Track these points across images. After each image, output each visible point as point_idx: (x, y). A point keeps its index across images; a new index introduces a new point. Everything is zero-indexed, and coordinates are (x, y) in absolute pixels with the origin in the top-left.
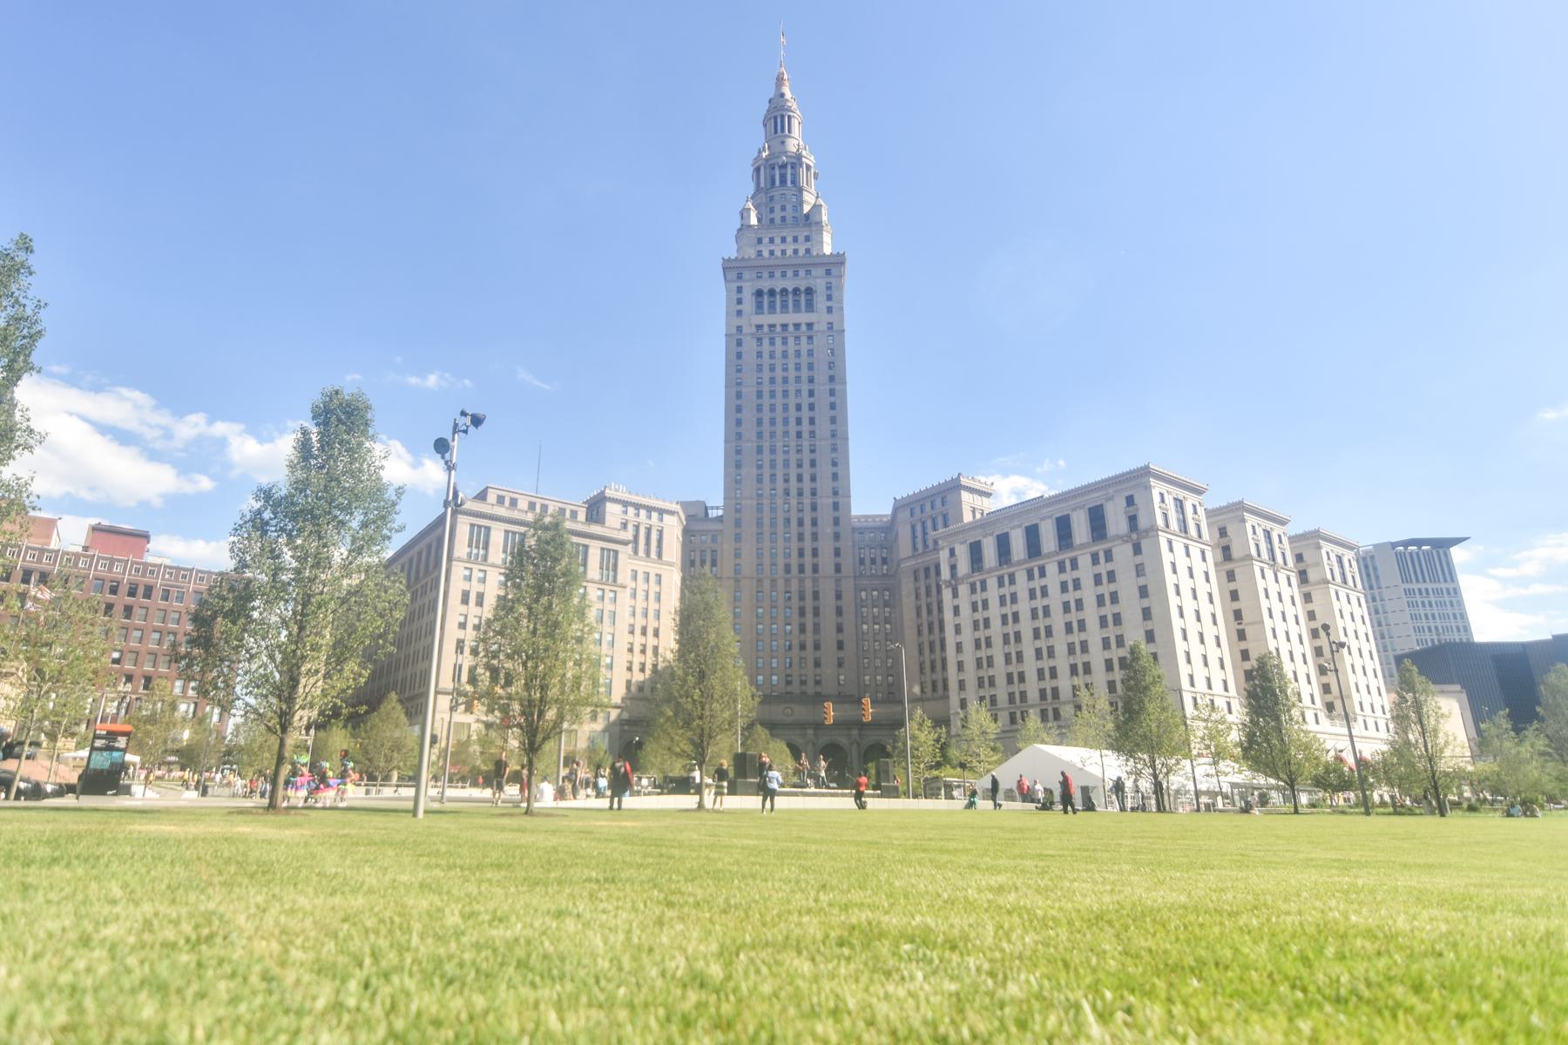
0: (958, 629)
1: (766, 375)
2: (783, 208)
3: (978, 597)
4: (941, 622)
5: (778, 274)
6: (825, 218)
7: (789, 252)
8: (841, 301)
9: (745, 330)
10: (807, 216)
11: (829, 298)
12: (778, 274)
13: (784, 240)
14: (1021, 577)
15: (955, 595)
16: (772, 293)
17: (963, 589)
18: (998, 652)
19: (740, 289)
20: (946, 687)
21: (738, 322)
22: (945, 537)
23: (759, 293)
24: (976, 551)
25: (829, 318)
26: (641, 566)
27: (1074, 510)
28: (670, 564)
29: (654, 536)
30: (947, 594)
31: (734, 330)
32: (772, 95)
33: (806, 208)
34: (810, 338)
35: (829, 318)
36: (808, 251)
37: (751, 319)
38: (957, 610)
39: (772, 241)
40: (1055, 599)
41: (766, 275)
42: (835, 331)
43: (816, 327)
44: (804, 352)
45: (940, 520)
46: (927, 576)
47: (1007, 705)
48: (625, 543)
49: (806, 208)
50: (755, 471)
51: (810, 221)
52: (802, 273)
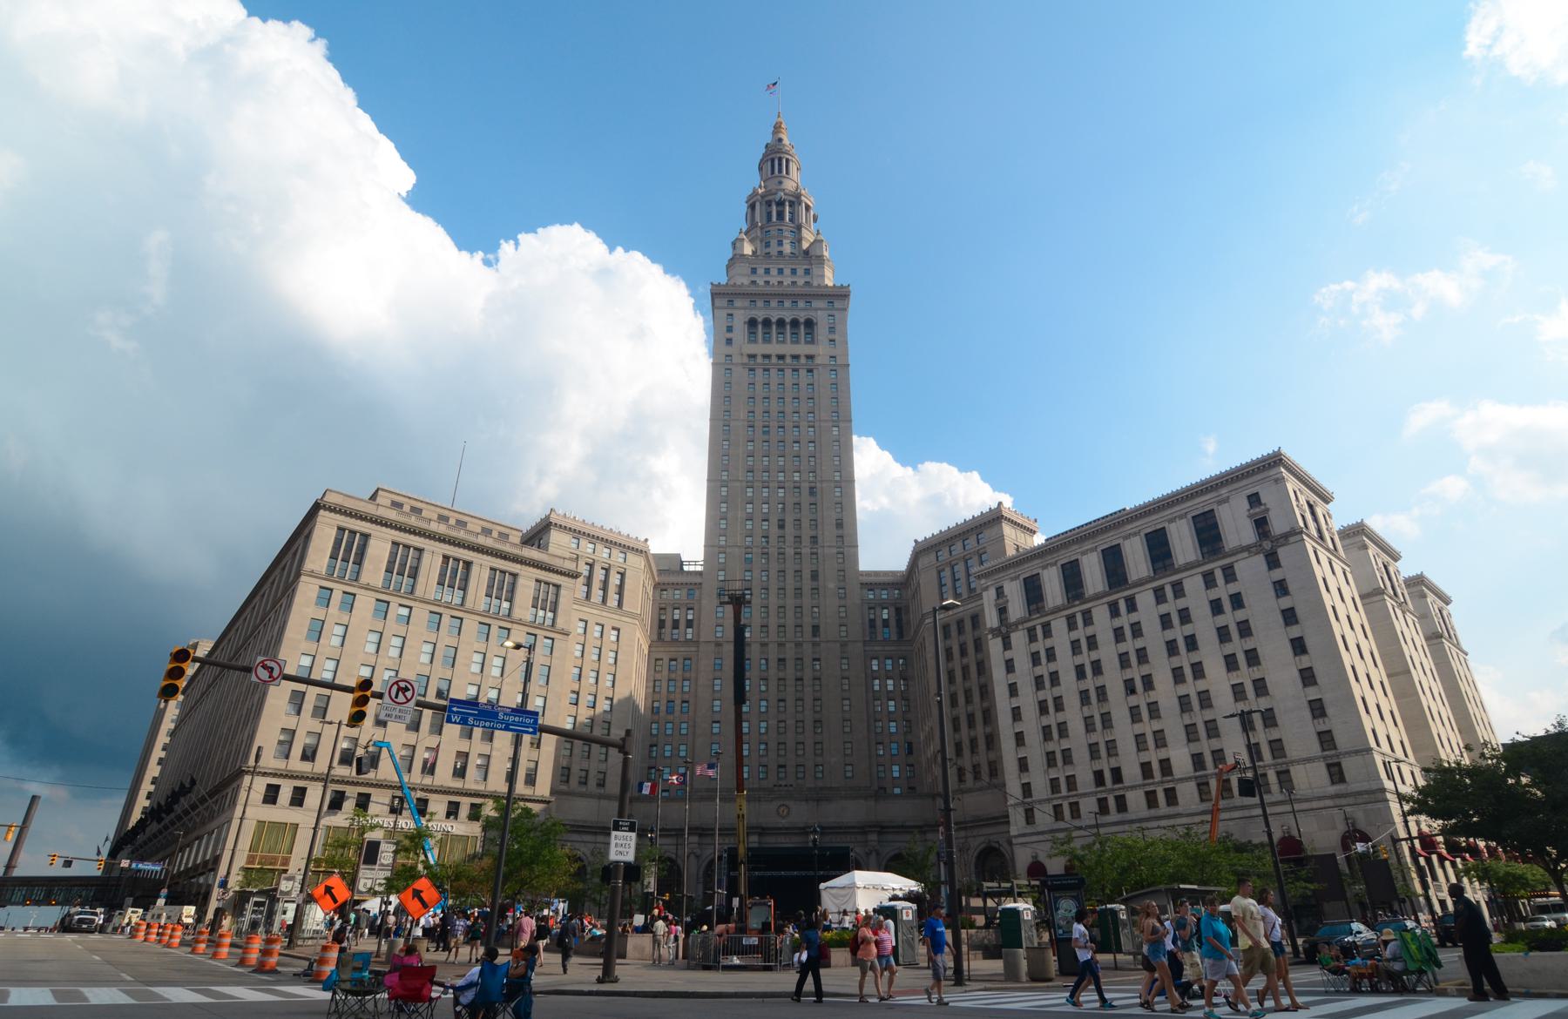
0: (1013, 690)
2: (780, 243)
3: (1040, 646)
5: (774, 303)
6: (826, 254)
9: (736, 359)
10: (806, 252)
11: (832, 330)
12: (774, 303)
14: (1101, 614)
15: (1007, 645)
16: (767, 323)
17: (1019, 638)
18: (1073, 715)
21: (729, 350)
22: (987, 575)
23: (752, 323)
24: (1033, 590)
26: (593, 613)
27: (1171, 521)
28: (632, 615)
29: (615, 580)
30: (995, 646)
31: (722, 360)
32: (769, 139)
33: (805, 245)
34: (810, 371)
38: (1010, 668)
39: (767, 271)
40: (1154, 639)
41: (760, 303)
42: (839, 367)
43: (818, 361)
44: (803, 385)
45: (974, 561)
46: (961, 630)
47: (1093, 789)
48: (574, 575)
49: (805, 245)
51: (811, 258)
52: (801, 304)
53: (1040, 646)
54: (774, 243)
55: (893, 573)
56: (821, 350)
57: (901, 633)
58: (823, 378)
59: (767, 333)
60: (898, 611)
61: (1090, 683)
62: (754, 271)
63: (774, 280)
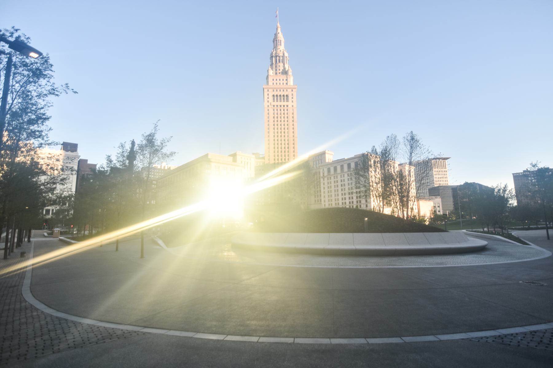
4: (320, 185)
7: (281, 84)
9: (270, 106)
12: (278, 90)
13: (280, 80)
14: (339, 177)
15: (324, 180)
16: (277, 96)
17: (326, 179)
18: (333, 194)
19: (268, 95)
20: (321, 201)
22: (322, 166)
23: (273, 96)
30: (322, 180)
36: (287, 84)
50: (273, 146)
52: (285, 90)
53: (329, 181)
56: (290, 104)
59: (277, 99)
61: (336, 189)
62: (273, 80)
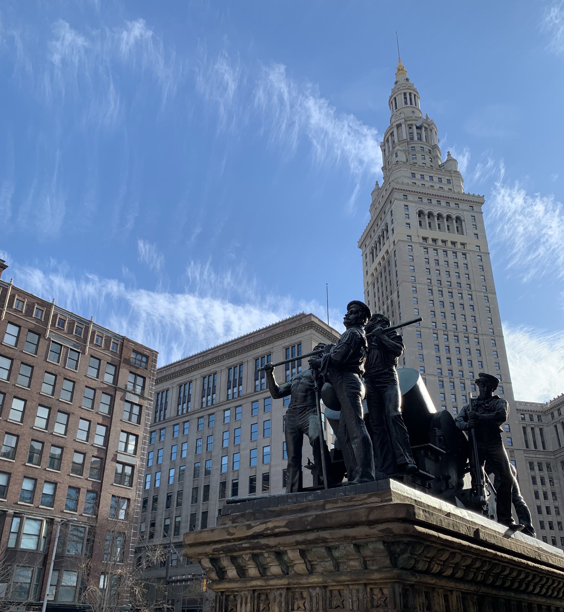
1: (434, 276)
5: (434, 202)
8: (484, 231)
12: (434, 202)
16: (430, 215)
23: (420, 213)
25: (477, 242)
31: (406, 238)
34: (464, 254)
35: (477, 242)
37: (418, 233)
41: (425, 200)
43: (468, 247)
44: (461, 264)
50: (433, 353)
51: (449, 171)
54: (419, 156)
55: (536, 404)
56: (468, 238)
57: (544, 448)
58: (472, 259)
60: (541, 430)
62: (413, 174)
63: (428, 184)
